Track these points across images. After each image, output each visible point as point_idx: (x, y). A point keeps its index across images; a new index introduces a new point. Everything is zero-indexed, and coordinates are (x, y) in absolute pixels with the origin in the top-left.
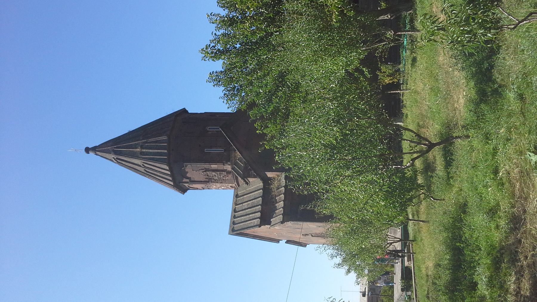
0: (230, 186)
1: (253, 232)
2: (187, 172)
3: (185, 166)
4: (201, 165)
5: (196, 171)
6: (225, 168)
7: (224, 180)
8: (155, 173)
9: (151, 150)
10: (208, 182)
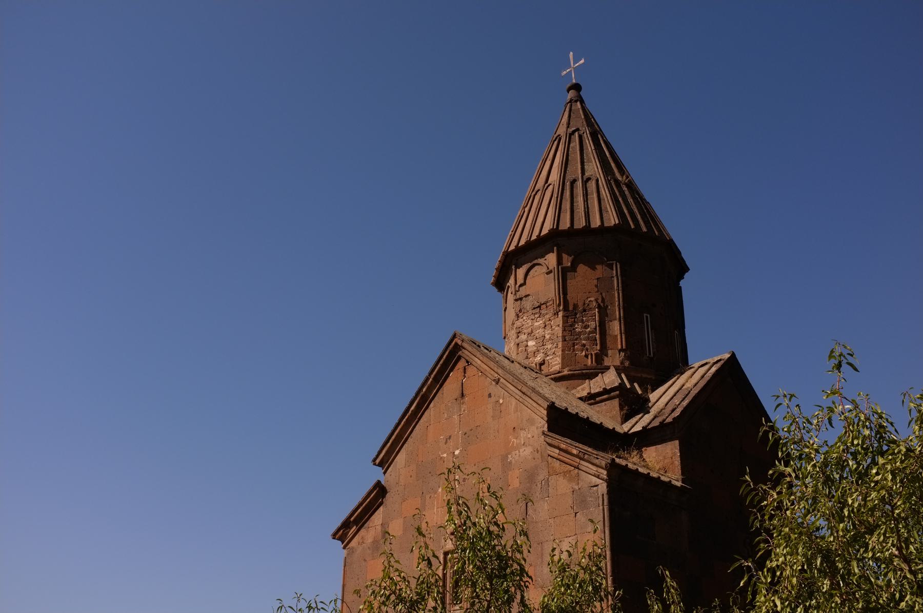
0: (544, 360)
1: (463, 395)
2: (594, 269)
3: (613, 264)
4: (617, 299)
5: (596, 286)
6: (610, 352)
7: (574, 346)
8: (580, 199)
9: (631, 200)
10: (566, 309)
